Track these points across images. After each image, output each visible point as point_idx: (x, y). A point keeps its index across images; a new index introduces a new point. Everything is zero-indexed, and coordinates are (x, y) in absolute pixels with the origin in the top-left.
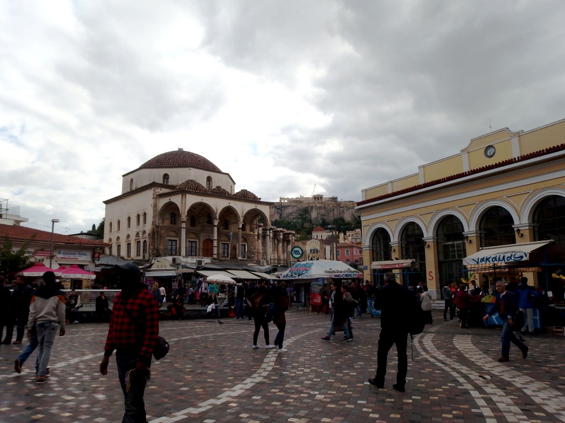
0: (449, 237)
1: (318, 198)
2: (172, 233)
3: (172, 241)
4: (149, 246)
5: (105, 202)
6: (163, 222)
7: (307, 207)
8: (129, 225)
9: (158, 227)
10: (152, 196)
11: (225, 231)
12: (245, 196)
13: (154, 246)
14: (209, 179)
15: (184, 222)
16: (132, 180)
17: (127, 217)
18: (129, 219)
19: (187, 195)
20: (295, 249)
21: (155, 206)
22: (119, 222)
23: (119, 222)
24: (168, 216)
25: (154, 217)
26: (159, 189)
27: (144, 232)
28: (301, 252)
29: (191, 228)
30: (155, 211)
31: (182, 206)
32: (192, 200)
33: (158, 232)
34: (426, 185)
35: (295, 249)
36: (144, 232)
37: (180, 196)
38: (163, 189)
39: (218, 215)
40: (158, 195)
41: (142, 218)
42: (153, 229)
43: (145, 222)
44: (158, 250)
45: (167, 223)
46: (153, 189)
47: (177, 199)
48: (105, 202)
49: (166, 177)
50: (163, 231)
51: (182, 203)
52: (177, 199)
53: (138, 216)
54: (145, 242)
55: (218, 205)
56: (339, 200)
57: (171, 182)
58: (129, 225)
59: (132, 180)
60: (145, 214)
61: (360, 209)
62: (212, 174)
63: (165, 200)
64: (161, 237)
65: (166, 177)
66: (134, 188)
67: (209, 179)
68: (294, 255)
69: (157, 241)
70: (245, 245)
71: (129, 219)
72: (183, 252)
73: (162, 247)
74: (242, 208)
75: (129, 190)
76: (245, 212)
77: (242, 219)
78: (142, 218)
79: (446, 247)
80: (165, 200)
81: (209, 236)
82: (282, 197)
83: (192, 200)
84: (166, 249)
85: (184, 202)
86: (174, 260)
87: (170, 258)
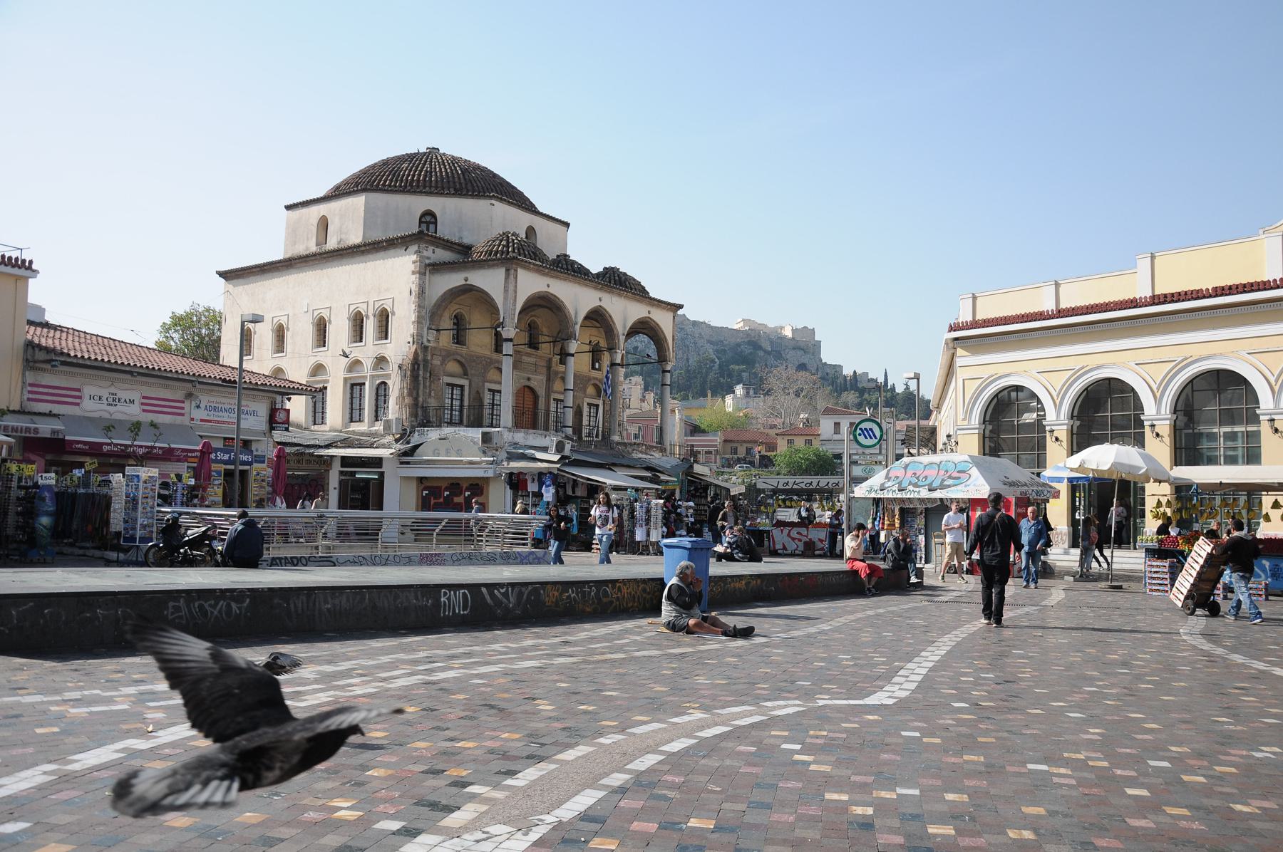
2: (453, 367)
3: (453, 386)
4: (402, 396)
5: (222, 274)
6: (437, 339)
9: (426, 348)
10: (412, 267)
11: (562, 368)
12: (615, 280)
13: (416, 399)
14: (531, 231)
15: (511, 340)
16: (324, 224)
19: (519, 270)
20: (863, 426)
21: (422, 292)
24: (447, 323)
25: (419, 321)
26: (431, 248)
27: (381, 361)
28: (878, 433)
29: (496, 356)
30: (420, 306)
31: (505, 298)
32: (530, 283)
33: (425, 361)
34: (1156, 300)
35: (863, 426)
36: (381, 361)
37: (500, 273)
38: (438, 251)
39: (578, 327)
40: (429, 265)
41: (370, 327)
42: (416, 353)
43: (384, 332)
44: (425, 409)
45: (446, 339)
46: (415, 247)
47: (490, 281)
48: (222, 274)
49: (429, 218)
50: (437, 362)
51: (506, 290)
52: (490, 281)
55: (578, 300)
57: (444, 231)
59: (324, 224)
60: (384, 318)
61: (956, 339)
62: (537, 222)
63: (454, 280)
64: (432, 375)
65: (429, 218)
66: (332, 244)
67: (531, 231)
68: (861, 439)
69: (425, 387)
70: (597, 406)
72: (507, 416)
73: (433, 403)
74: (624, 312)
75: (313, 248)
76: (629, 324)
77: (622, 338)
78: (370, 327)
80: (454, 280)
81: (529, 379)
83: (530, 283)
84: (441, 408)
85: (511, 288)
86: (486, 438)
87: (476, 434)
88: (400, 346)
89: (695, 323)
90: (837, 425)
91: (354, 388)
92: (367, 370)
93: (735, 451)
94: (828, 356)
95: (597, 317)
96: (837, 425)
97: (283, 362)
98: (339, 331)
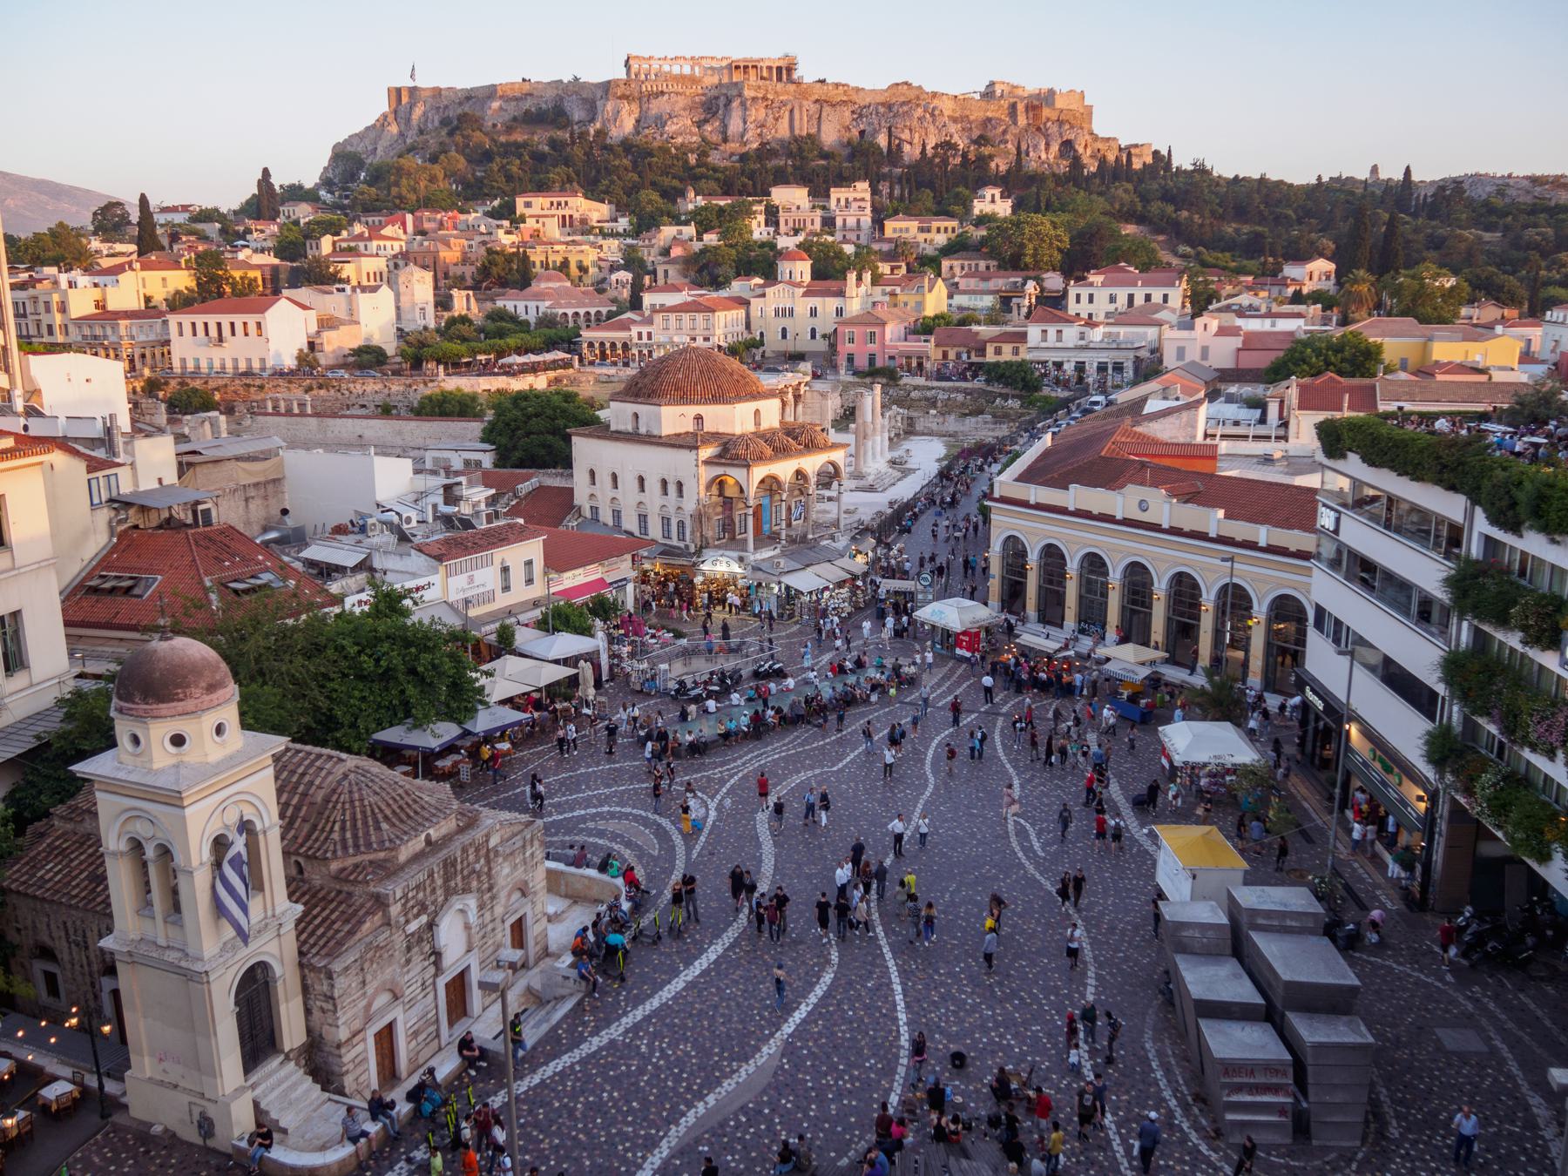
0: (1091, 572)
1: (746, 67)
4: (693, 533)
7: (717, 98)
8: (642, 489)
16: (636, 416)
17: (636, 474)
18: (641, 480)
22: (615, 477)
23: (615, 477)
32: (759, 472)
41: (672, 489)
49: (699, 418)
53: (664, 483)
54: (681, 524)
56: (807, 73)
57: (708, 427)
58: (642, 489)
59: (636, 416)
60: (680, 485)
65: (699, 418)
71: (641, 480)
75: (630, 428)
78: (672, 489)
79: (1089, 581)
80: (719, 471)
82: (634, 54)
88: (689, 505)
89: (934, 95)
90: (1045, 332)
91: (666, 521)
92: (672, 510)
93: (945, 355)
94: (1101, 127)
95: (800, 474)
96: (1045, 332)
97: (618, 494)
98: (653, 485)
